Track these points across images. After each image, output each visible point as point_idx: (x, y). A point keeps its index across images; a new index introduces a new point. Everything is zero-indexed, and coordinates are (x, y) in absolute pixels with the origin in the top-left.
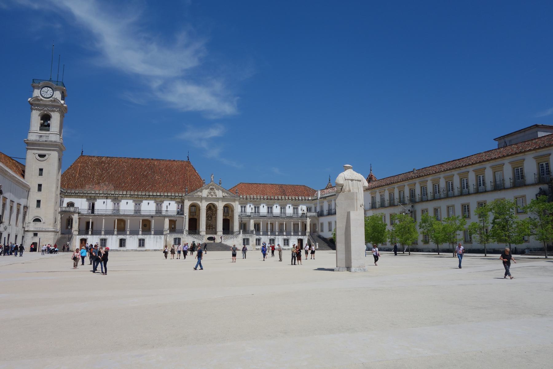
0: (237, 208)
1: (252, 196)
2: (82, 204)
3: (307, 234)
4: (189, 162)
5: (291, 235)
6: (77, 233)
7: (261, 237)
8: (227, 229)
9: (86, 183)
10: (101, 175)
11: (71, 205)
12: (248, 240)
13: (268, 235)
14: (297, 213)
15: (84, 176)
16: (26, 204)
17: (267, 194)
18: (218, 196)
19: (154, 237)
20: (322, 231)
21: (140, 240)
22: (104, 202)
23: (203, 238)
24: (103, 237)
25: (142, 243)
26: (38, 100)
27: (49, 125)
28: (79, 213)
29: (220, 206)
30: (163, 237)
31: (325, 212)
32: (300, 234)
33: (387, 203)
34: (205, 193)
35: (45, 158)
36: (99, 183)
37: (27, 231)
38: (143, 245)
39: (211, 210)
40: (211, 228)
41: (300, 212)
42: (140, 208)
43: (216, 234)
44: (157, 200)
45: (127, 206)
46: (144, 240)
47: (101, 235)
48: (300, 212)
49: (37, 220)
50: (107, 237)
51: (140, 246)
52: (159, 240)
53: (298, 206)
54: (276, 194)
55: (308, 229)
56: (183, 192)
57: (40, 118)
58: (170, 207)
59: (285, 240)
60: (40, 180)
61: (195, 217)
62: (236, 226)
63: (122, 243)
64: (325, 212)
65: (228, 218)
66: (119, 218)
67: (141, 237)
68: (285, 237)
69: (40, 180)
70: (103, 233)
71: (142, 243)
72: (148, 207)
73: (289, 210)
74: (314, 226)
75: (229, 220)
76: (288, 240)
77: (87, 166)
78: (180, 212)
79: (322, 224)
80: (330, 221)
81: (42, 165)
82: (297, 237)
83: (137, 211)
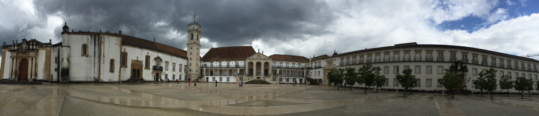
0: (271, 64)
23: (255, 78)
28: (206, 68)
29: (263, 63)
39: (259, 64)
43: (260, 75)
45: (224, 64)
55: (305, 74)
62: (270, 72)
72: (232, 64)
74: (307, 73)
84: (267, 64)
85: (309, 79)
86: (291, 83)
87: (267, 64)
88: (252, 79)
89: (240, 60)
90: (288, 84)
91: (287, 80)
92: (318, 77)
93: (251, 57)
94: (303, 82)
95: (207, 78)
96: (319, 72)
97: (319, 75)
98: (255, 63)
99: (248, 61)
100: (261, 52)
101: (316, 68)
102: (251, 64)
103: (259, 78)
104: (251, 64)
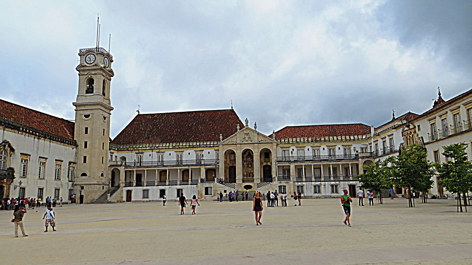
0: (277, 153)
2: (131, 157)
4: (232, 110)
5: (341, 181)
6: (124, 185)
7: (304, 183)
8: (267, 176)
9: (138, 139)
10: (151, 131)
11: (124, 158)
15: (137, 133)
16: (73, 160)
18: (253, 142)
22: (150, 155)
23: (239, 186)
24: (145, 188)
26: (83, 66)
27: (93, 88)
28: (126, 166)
35: (90, 117)
36: (149, 138)
37: (76, 185)
39: (248, 154)
40: (248, 176)
41: (353, 153)
45: (170, 156)
48: (353, 153)
49: (84, 175)
50: (148, 188)
53: (352, 145)
54: (324, 136)
57: (85, 82)
58: (209, 154)
60: (86, 138)
63: (162, 193)
65: (269, 164)
69: (86, 138)
70: (145, 184)
72: (189, 156)
73: (339, 152)
76: (336, 186)
77: (142, 124)
81: (87, 123)
86: (326, 197)
87: (266, 154)
89: (206, 146)
95: (129, 192)
101: (384, 154)
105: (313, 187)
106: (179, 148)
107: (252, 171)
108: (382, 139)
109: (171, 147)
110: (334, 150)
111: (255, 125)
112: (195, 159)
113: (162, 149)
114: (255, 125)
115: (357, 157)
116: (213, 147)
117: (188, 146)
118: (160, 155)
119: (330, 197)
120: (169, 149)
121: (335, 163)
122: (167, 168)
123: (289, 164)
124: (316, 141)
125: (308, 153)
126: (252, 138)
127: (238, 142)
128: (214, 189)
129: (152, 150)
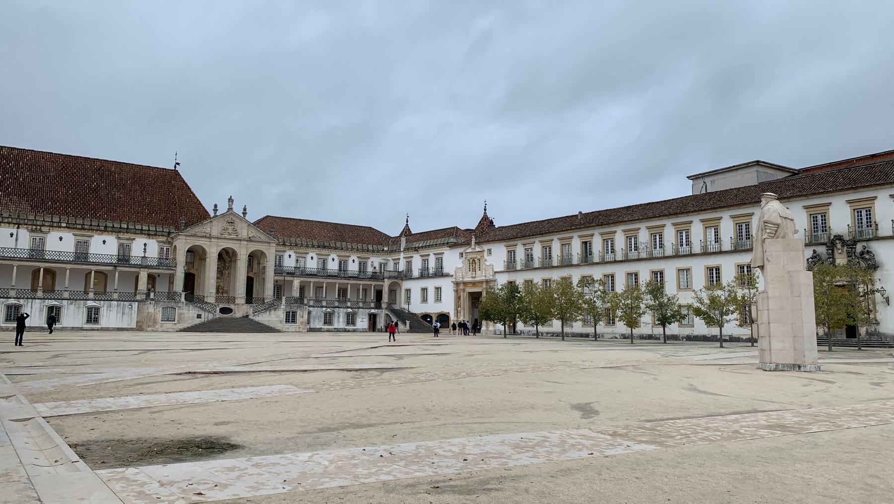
1: (293, 240)
3: (384, 306)
4: (176, 172)
5: (359, 308)
7: (311, 309)
12: (294, 314)
13: (322, 307)
14: (365, 272)
17: (315, 238)
19: (118, 306)
20: (408, 299)
21: (90, 309)
22: (12, 235)
24: (12, 301)
25: (93, 316)
30: (135, 305)
31: (416, 273)
32: (372, 305)
33: (537, 264)
34: (215, 228)
38: (96, 321)
39: (226, 258)
41: (370, 269)
42: (87, 249)
43: (233, 300)
44: (121, 235)
45: (60, 242)
46: (97, 309)
47: (7, 298)
48: (370, 269)
50: (22, 302)
51: (89, 321)
52: (127, 310)
56: (169, 225)
58: (147, 248)
59: (348, 315)
61: (192, 271)
64: (416, 273)
65: (251, 275)
66: (47, 265)
67: (90, 303)
68: (350, 310)
70: (13, 293)
71: (93, 316)
72: (104, 246)
75: (252, 279)
78: (166, 261)
79: (408, 291)
80: (424, 286)
82: (367, 311)
83: (81, 256)
84: (254, 258)
85: (403, 316)
86: (338, 330)
88: (211, 316)
89: (141, 232)
90: (328, 331)
91: (328, 319)
92: (433, 308)
93: (198, 229)
94: (381, 323)
96: (438, 289)
97: (438, 299)
98: (213, 252)
99: (183, 244)
100: (238, 209)
102: (196, 255)
103: (229, 311)
104: (196, 255)
105: (323, 315)
106: (83, 229)
107: (221, 284)
108: (421, 256)
109: (64, 225)
110: (346, 262)
111: (245, 209)
112: (115, 252)
113: (43, 226)
114: (245, 209)
115: (375, 277)
116: (155, 235)
117: (103, 228)
118: (38, 236)
119: (345, 331)
120: (60, 227)
121: (354, 282)
122: (69, 266)
123: (291, 278)
124: (325, 247)
125: (312, 263)
126: (239, 231)
127: (215, 232)
128: (181, 311)
129: (19, 224)
